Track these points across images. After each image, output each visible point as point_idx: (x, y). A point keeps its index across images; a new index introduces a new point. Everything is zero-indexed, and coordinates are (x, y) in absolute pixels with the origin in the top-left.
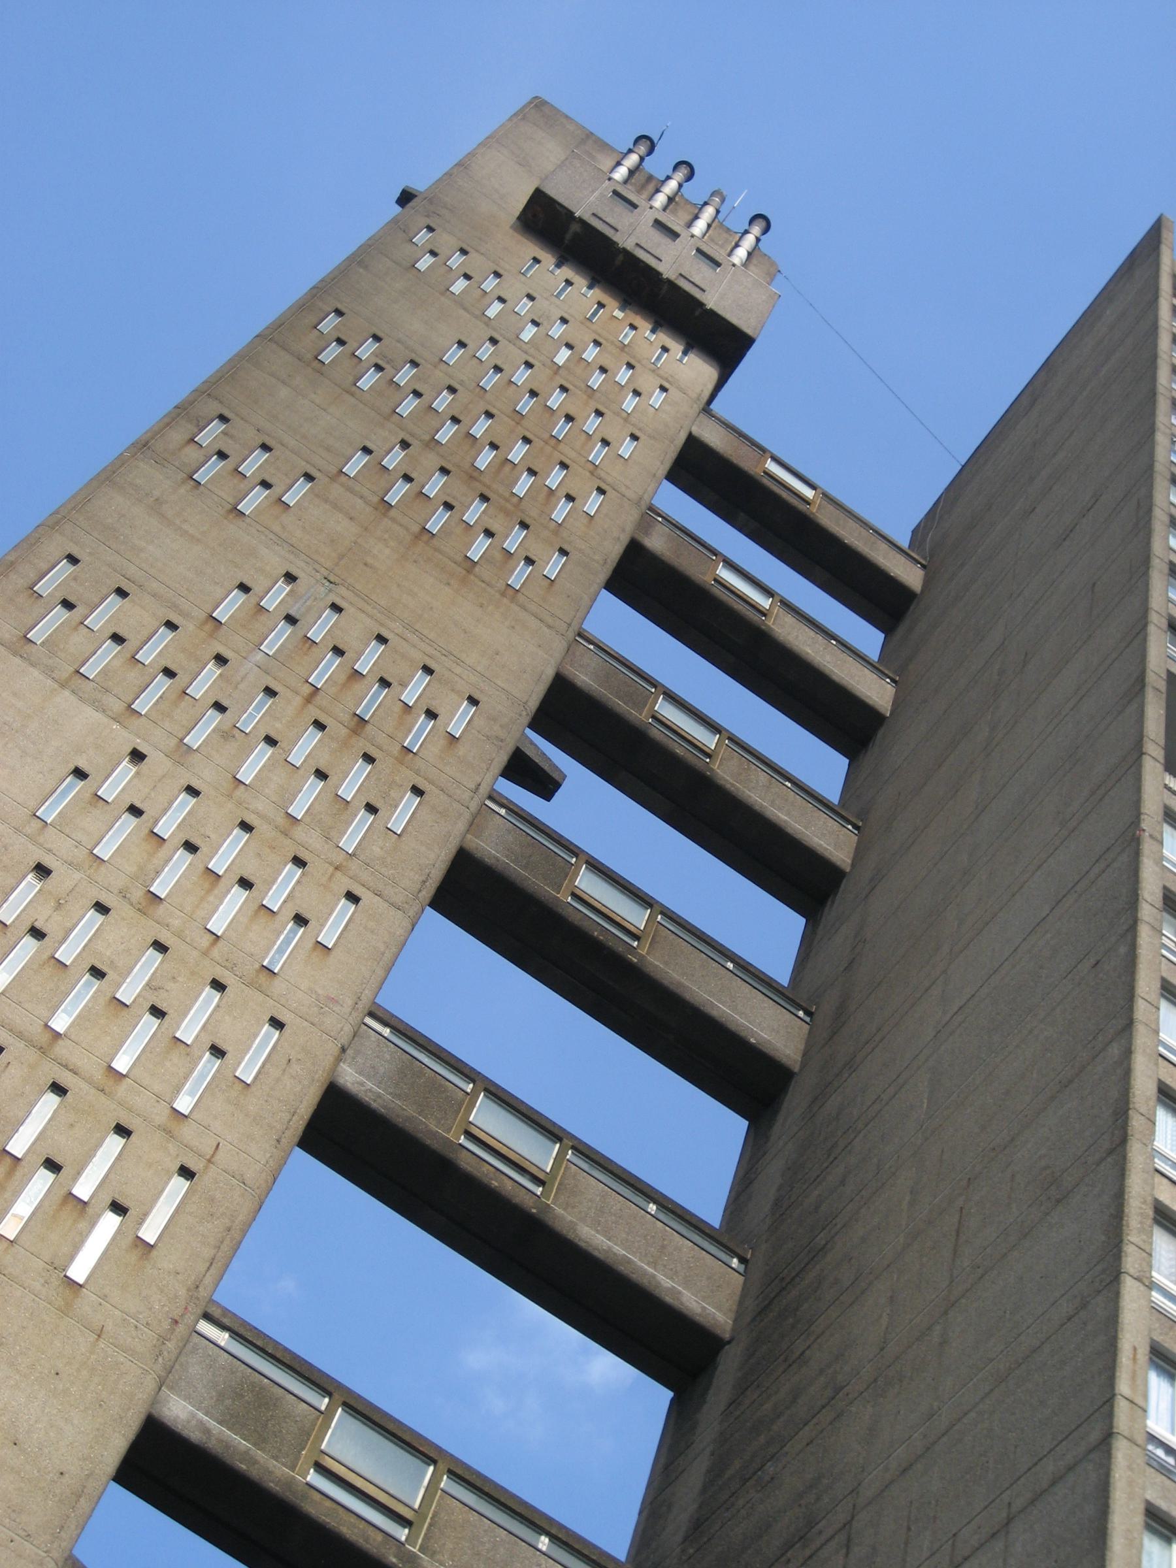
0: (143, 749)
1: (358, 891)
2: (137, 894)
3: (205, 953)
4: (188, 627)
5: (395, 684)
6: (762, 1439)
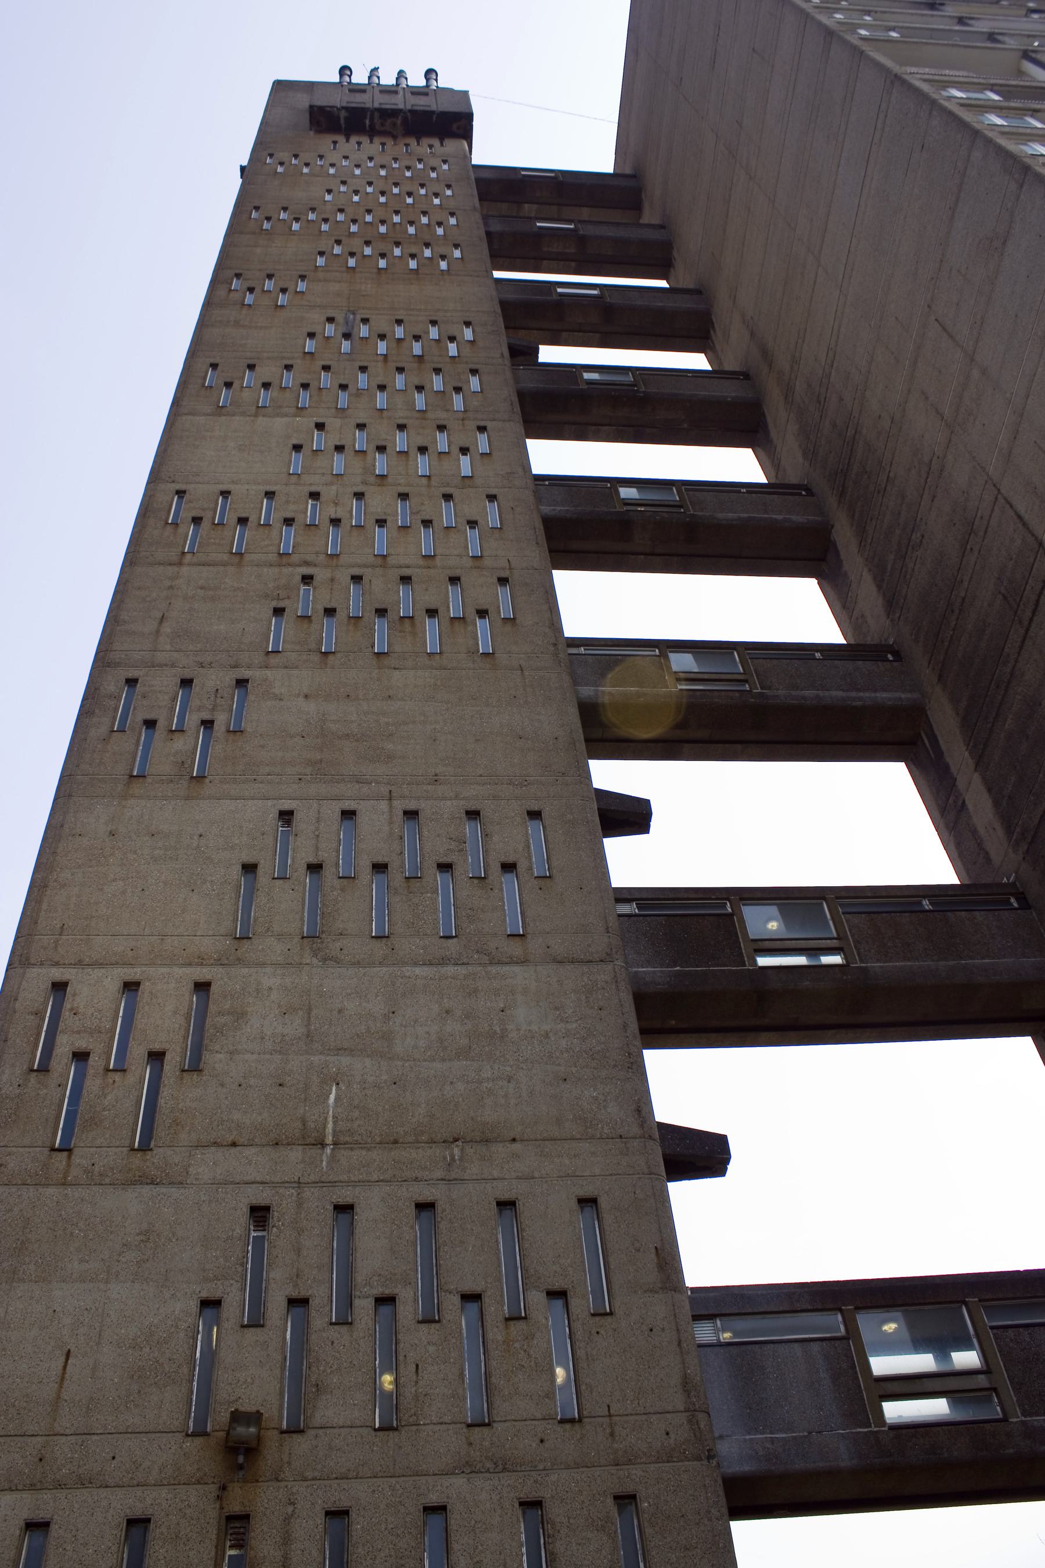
0: (320, 420)
1: (482, 424)
2: (372, 479)
4: (298, 363)
5: (422, 335)
6: (898, 532)
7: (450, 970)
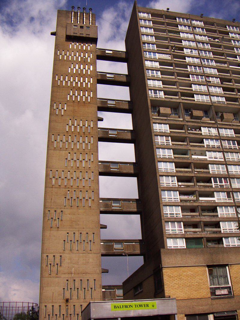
3: (84, 170)
7: (84, 254)
